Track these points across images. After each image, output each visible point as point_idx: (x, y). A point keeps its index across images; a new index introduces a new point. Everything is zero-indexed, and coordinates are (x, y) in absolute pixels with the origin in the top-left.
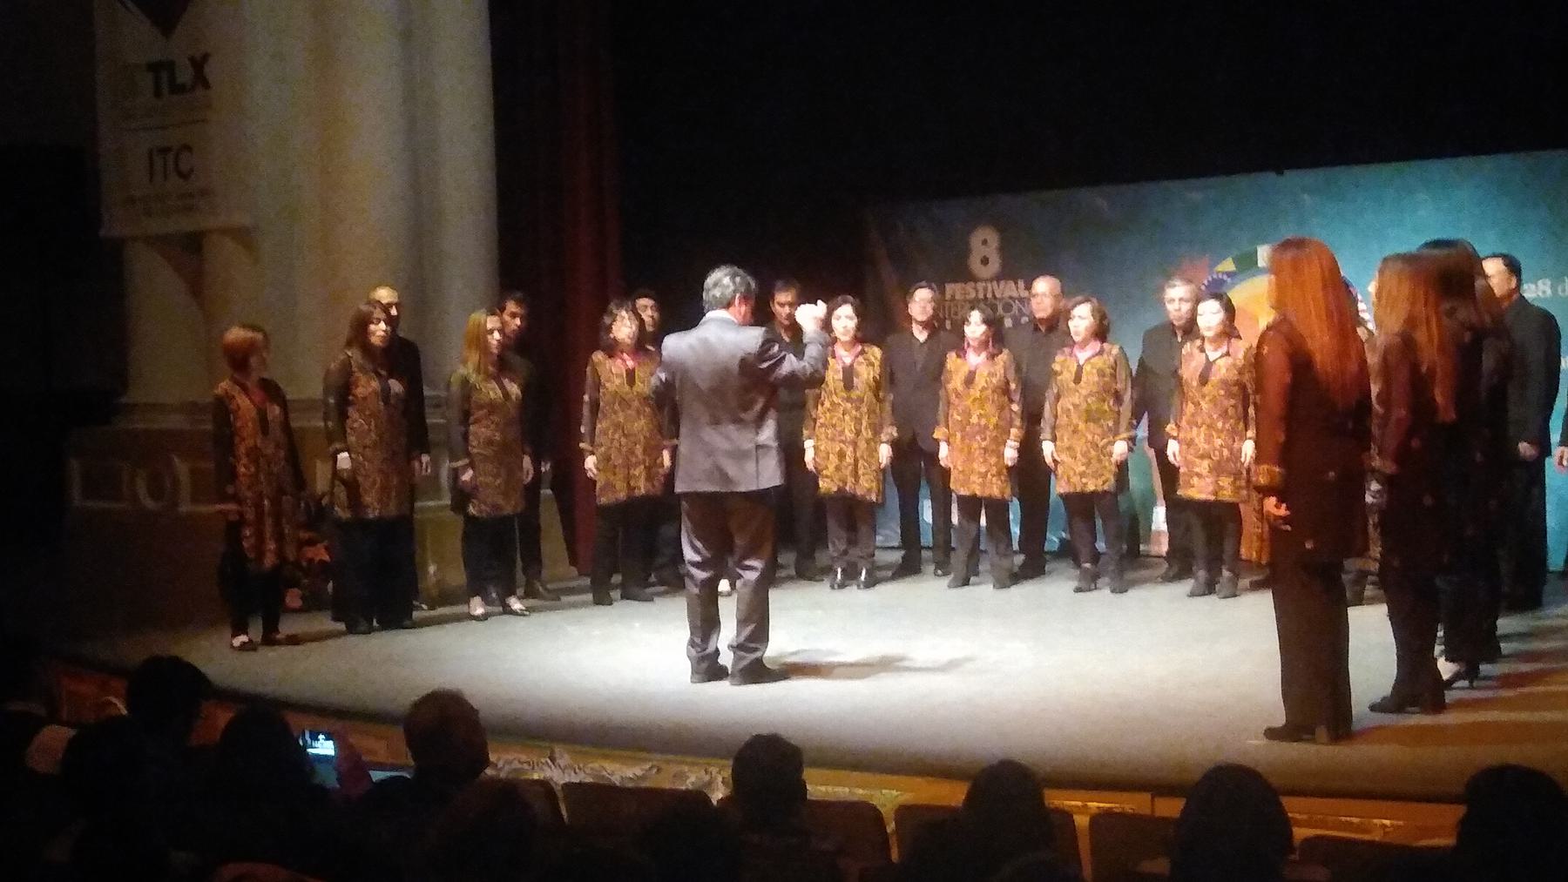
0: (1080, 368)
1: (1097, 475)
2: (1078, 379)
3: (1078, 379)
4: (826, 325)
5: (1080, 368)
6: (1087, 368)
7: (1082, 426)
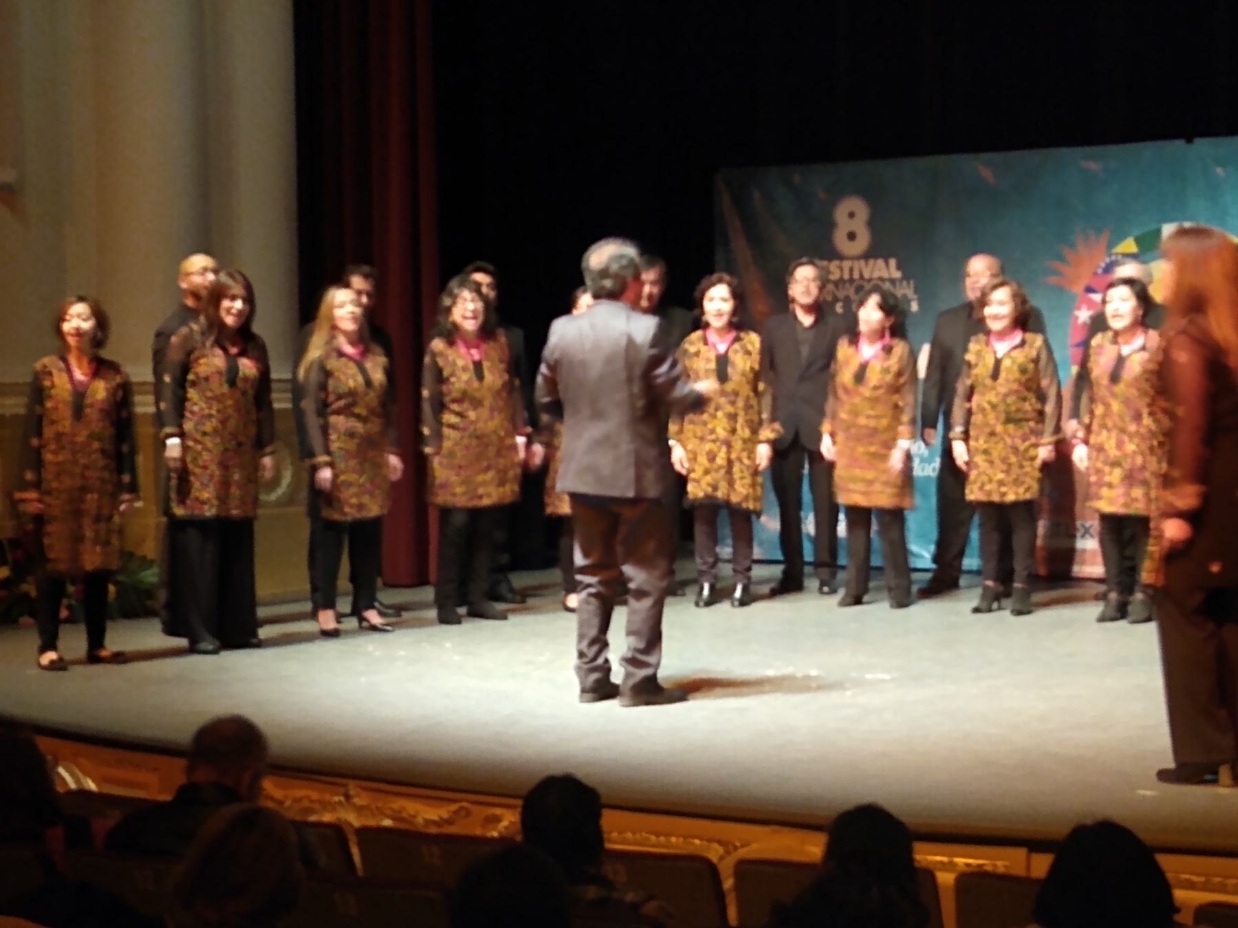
0: (998, 362)
1: (1017, 482)
2: (995, 375)
3: (995, 375)
5: (998, 362)
6: (1007, 363)
7: (999, 428)
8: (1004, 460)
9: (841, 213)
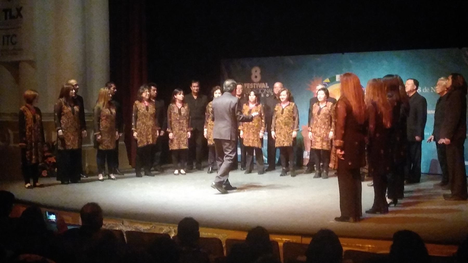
0: (283, 110)
2: (282, 113)
5: (283, 110)
6: (285, 110)
7: (283, 127)
8: (284, 135)
9: (253, 71)
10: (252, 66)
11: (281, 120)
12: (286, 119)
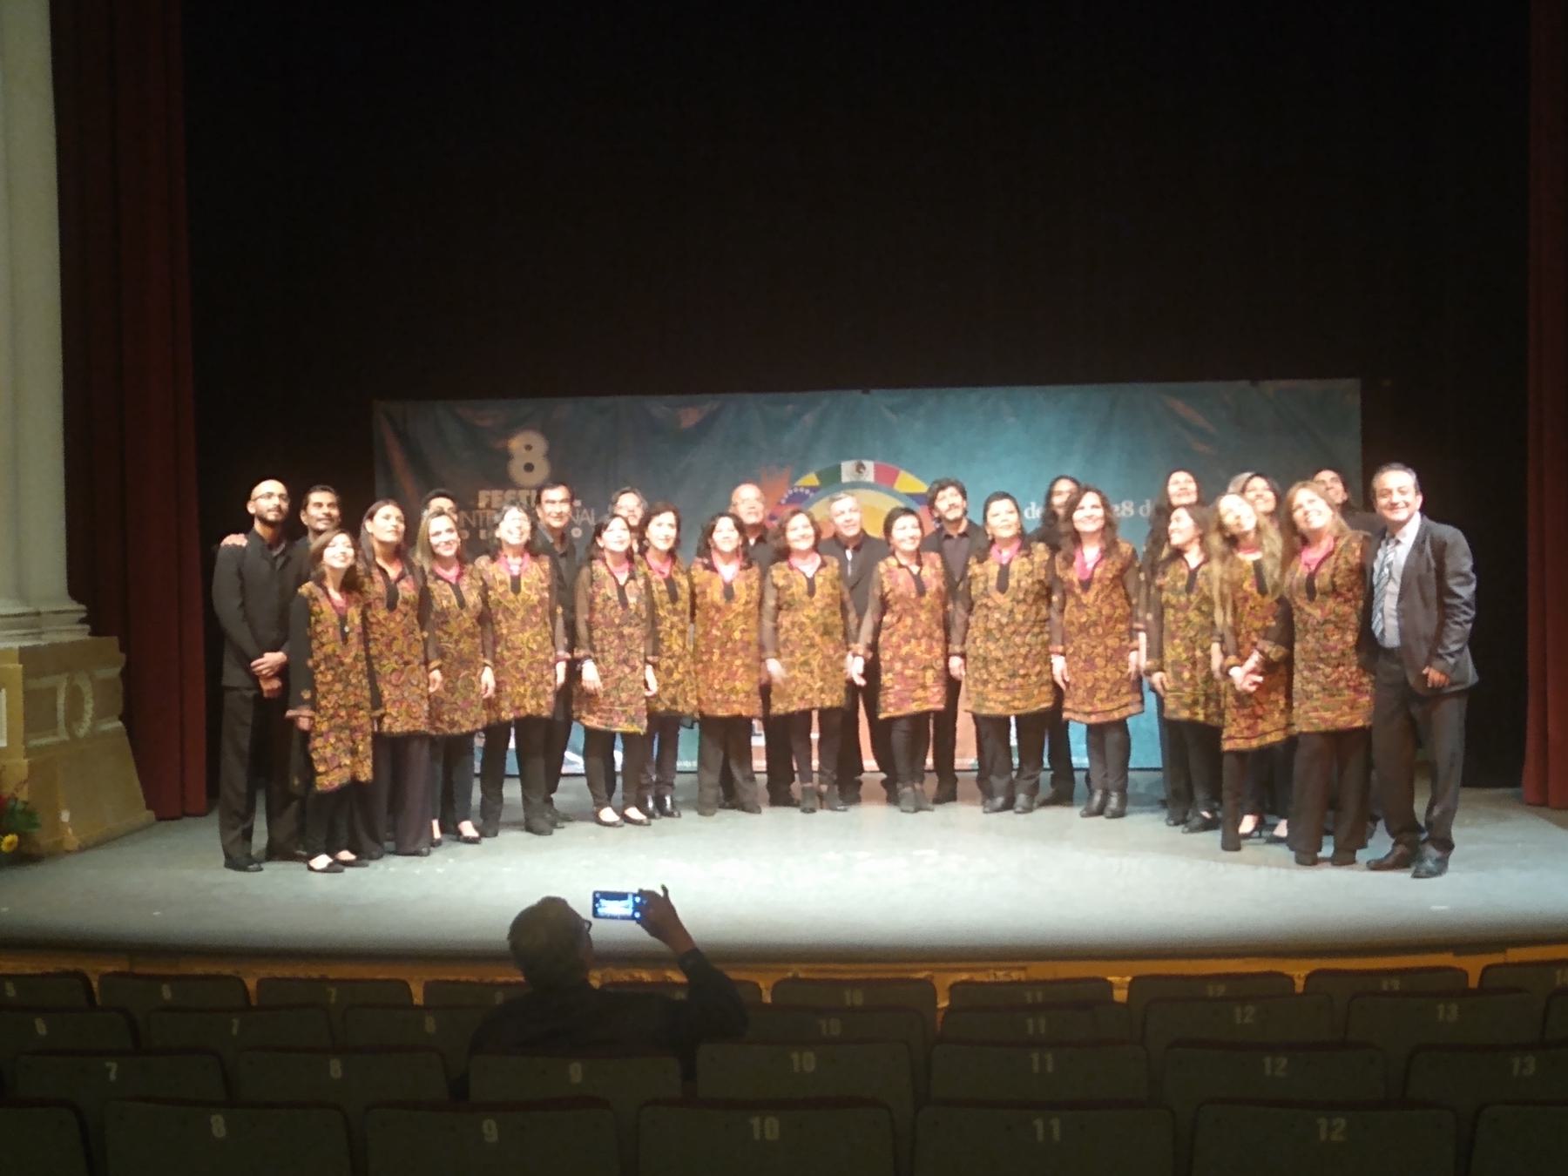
0: (811, 582)
2: (811, 591)
3: (811, 591)
4: (640, 531)
5: (811, 582)
6: (819, 581)
7: (818, 639)
8: (822, 668)
9: (516, 444)
10: (509, 430)
11: (808, 617)
12: (826, 612)
